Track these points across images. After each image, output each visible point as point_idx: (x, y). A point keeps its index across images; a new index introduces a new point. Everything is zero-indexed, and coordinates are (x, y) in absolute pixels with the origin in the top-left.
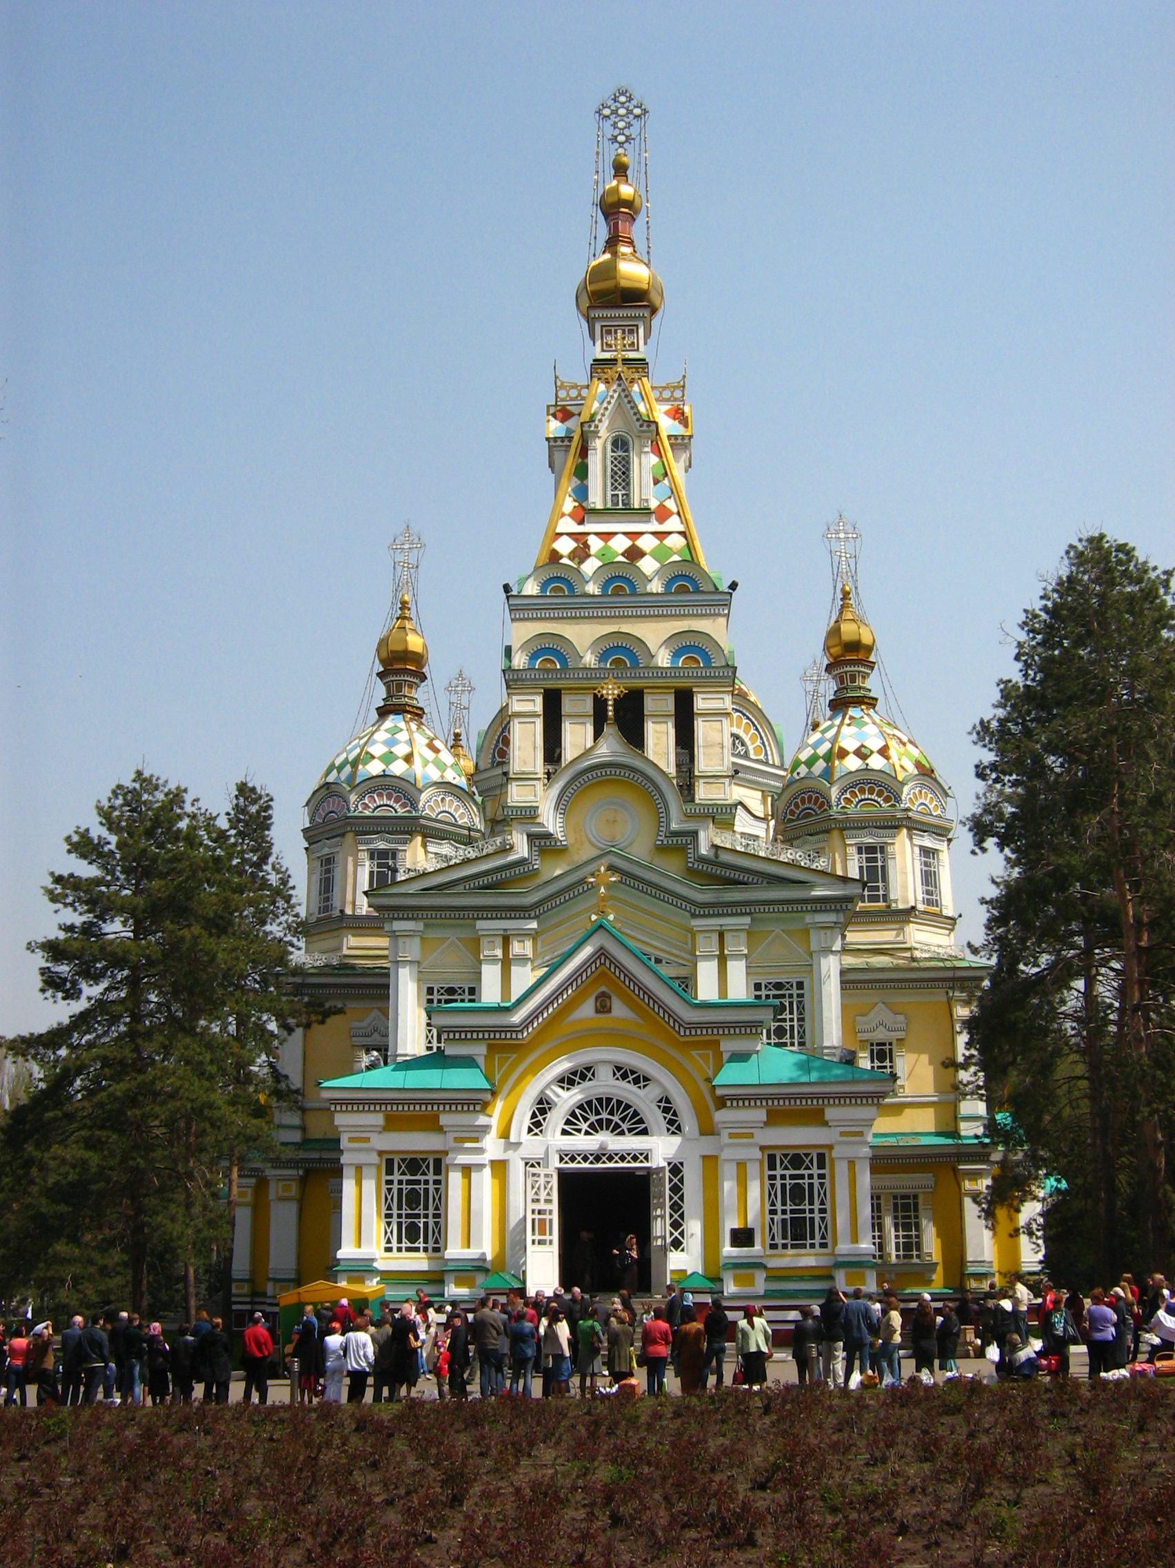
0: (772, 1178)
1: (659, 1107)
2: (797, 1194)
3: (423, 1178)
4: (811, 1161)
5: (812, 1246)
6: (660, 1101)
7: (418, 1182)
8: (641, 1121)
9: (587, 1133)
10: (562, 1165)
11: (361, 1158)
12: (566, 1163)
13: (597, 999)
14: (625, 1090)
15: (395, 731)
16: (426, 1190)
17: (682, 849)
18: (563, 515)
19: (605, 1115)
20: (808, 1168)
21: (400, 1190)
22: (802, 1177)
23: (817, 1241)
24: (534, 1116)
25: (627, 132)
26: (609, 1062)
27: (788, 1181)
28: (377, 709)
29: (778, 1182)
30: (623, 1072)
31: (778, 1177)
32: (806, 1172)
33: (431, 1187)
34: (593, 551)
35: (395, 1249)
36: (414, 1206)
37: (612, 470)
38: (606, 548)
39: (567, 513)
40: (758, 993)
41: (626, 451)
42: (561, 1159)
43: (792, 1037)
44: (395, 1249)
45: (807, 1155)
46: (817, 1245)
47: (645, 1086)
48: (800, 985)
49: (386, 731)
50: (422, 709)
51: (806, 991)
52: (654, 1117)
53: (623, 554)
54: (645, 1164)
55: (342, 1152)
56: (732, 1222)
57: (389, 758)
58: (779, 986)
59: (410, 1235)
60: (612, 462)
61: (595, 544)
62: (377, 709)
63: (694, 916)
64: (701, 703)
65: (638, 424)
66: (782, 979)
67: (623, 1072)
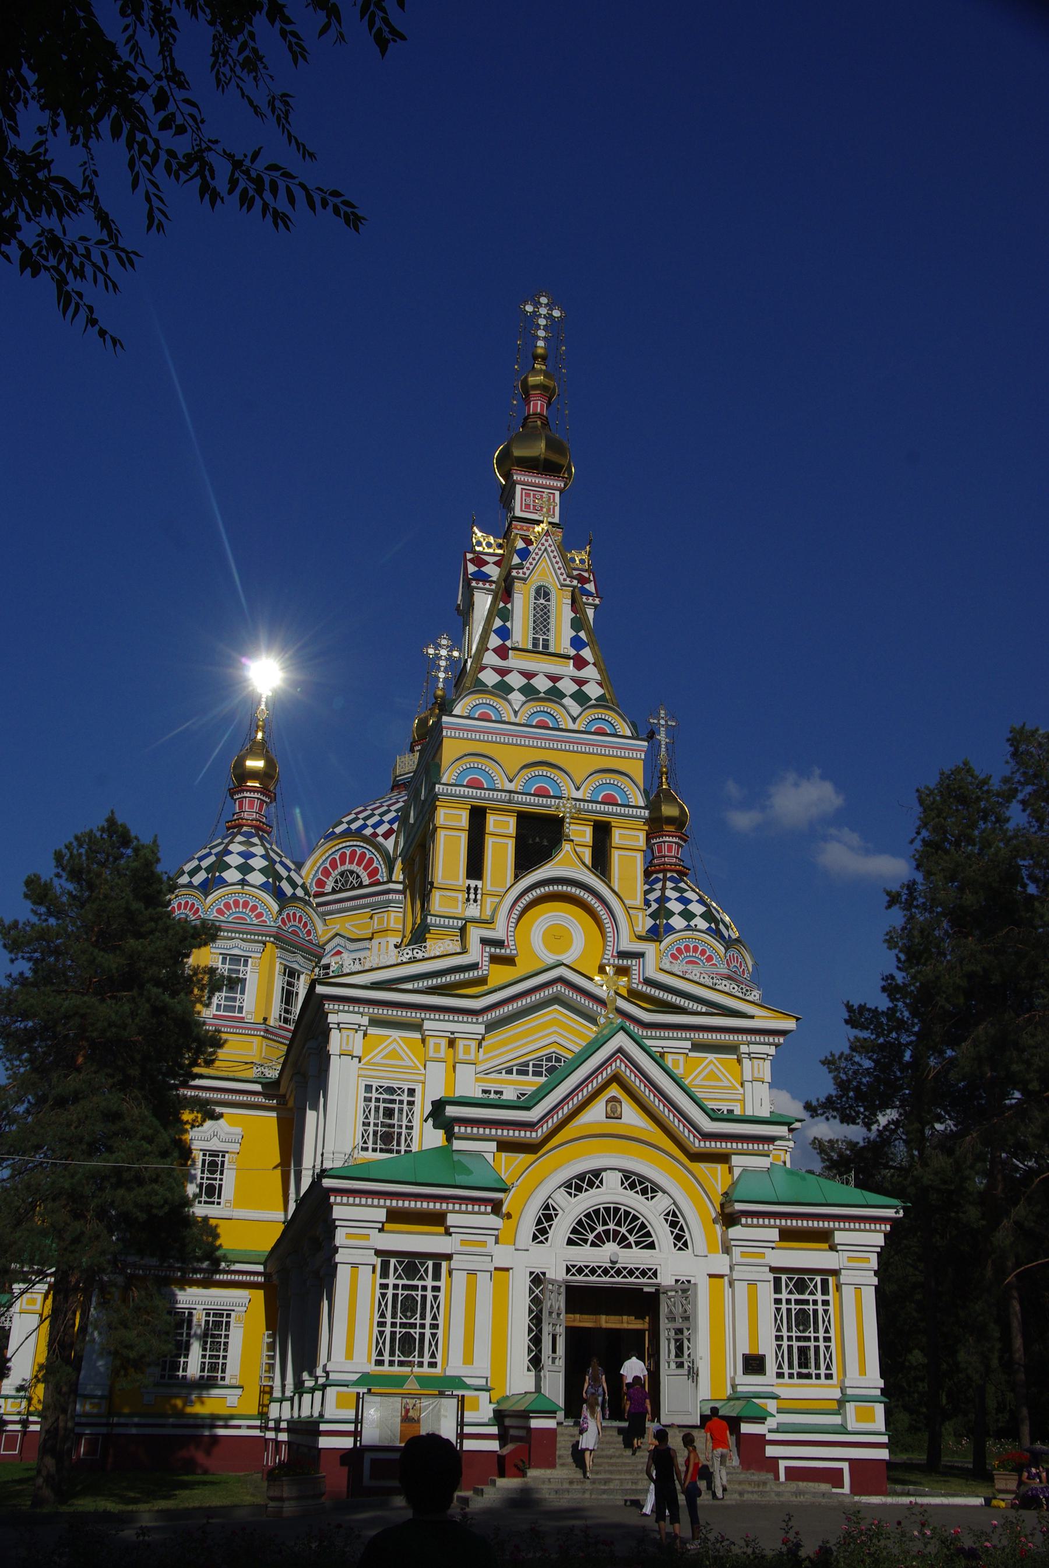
0: (778, 1301)
1: (666, 1220)
2: (803, 1319)
3: (420, 1283)
4: (815, 1286)
5: (818, 1376)
6: (668, 1214)
7: (415, 1288)
8: (648, 1234)
9: (593, 1244)
10: (569, 1277)
11: (356, 1256)
12: (573, 1274)
14: (633, 1201)
16: (424, 1297)
18: (488, 649)
19: (612, 1226)
20: (811, 1293)
21: (395, 1296)
22: (807, 1302)
23: (823, 1371)
24: (539, 1222)
26: (620, 1170)
27: (793, 1306)
29: (784, 1307)
30: (633, 1181)
31: (784, 1301)
32: (811, 1298)
33: (429, 1294)
35: (387, 1363)
36: (409, 1314)
41: (548, 600)
42: (568, 1270)
44: (387, 1363)
45: (811, 1280)
46: (823, 1376)
47: (652, 1198)
52: (662, 1233)
54: (654, 1281)
55: (336, 1250)
56: (744, 1348)
59: (403, 1347)
64: (617, 837)
67: (633, 1181)
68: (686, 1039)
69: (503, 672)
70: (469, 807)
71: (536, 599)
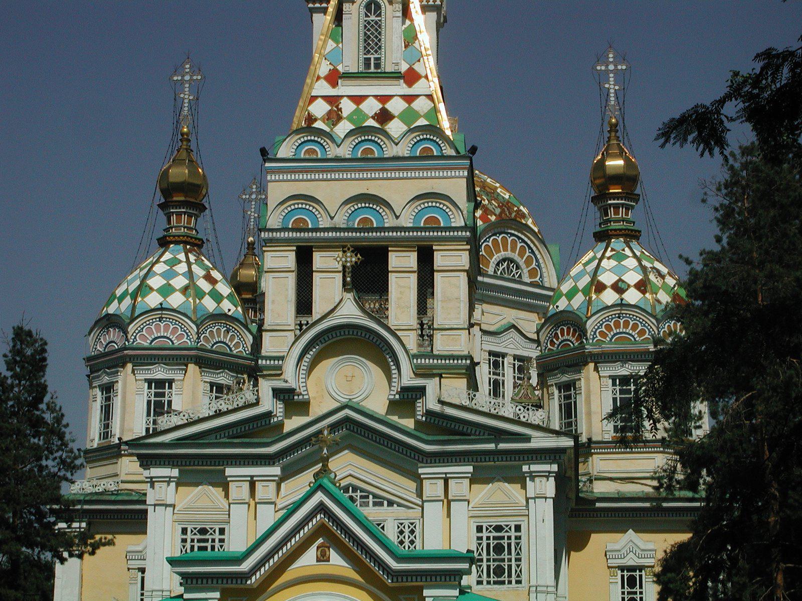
13: (318, 548)
15: (174, 262)
18: (319, 78)
28: (158, 240)
34: (345, 114)
37: (365, 34)
38: (358, 111)
39: (322, 75)
40: (480, 535)
41: (379, 15)
43: (510, 575)
48: (518, 528)
49: (164, 262)
50: (201, 240)
51: (523, 533)
53: (373, 117)
57: (166, 290)
58: (498, 528)
60: (365, 26)
61: (347, 107)
62: (158, 240)
64: (440, 260)
66: (501, 522)
69: (333, 100)
70: (295, 248)
71: (367, 16)
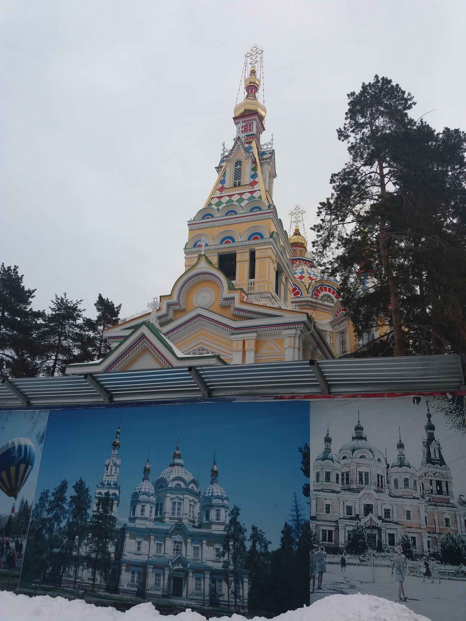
17: (229, 307)
25: (256, 60)
63: (233, 334)
64: (257, 255)
65: (245, 154)
68: (255, 332)
71: (236, 166)
